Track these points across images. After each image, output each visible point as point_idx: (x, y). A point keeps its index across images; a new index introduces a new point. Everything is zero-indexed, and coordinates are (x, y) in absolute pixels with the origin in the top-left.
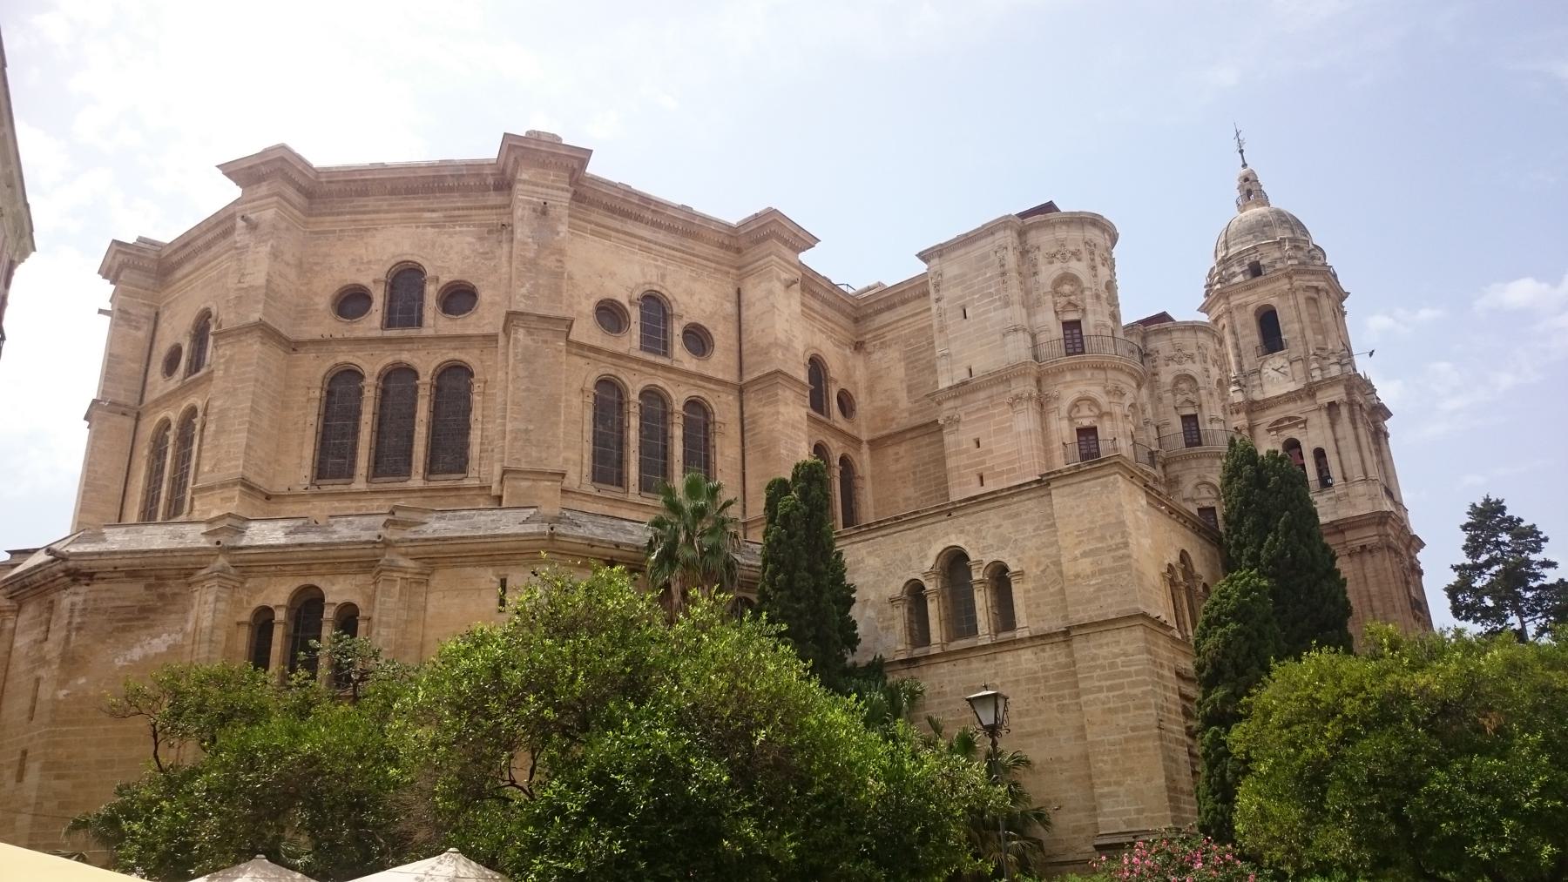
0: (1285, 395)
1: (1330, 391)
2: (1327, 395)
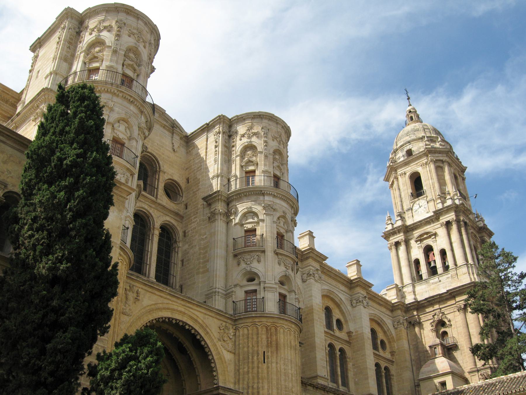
0: (424, 219)
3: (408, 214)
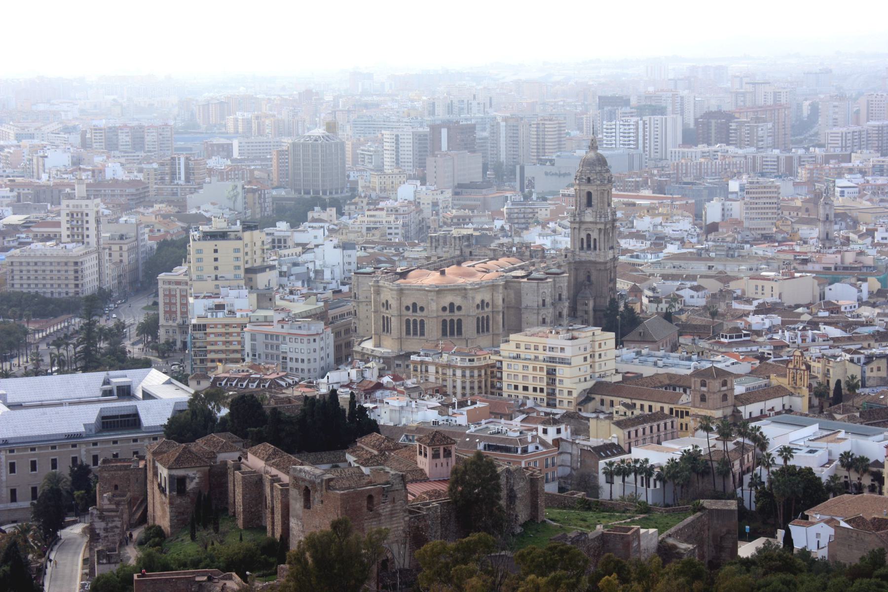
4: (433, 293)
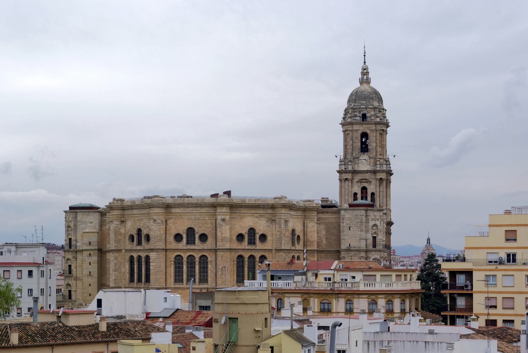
0: (366, 171)
1: (381, 174)
2: (380, 175)
3: (356, 161)
4: (224, 210)
